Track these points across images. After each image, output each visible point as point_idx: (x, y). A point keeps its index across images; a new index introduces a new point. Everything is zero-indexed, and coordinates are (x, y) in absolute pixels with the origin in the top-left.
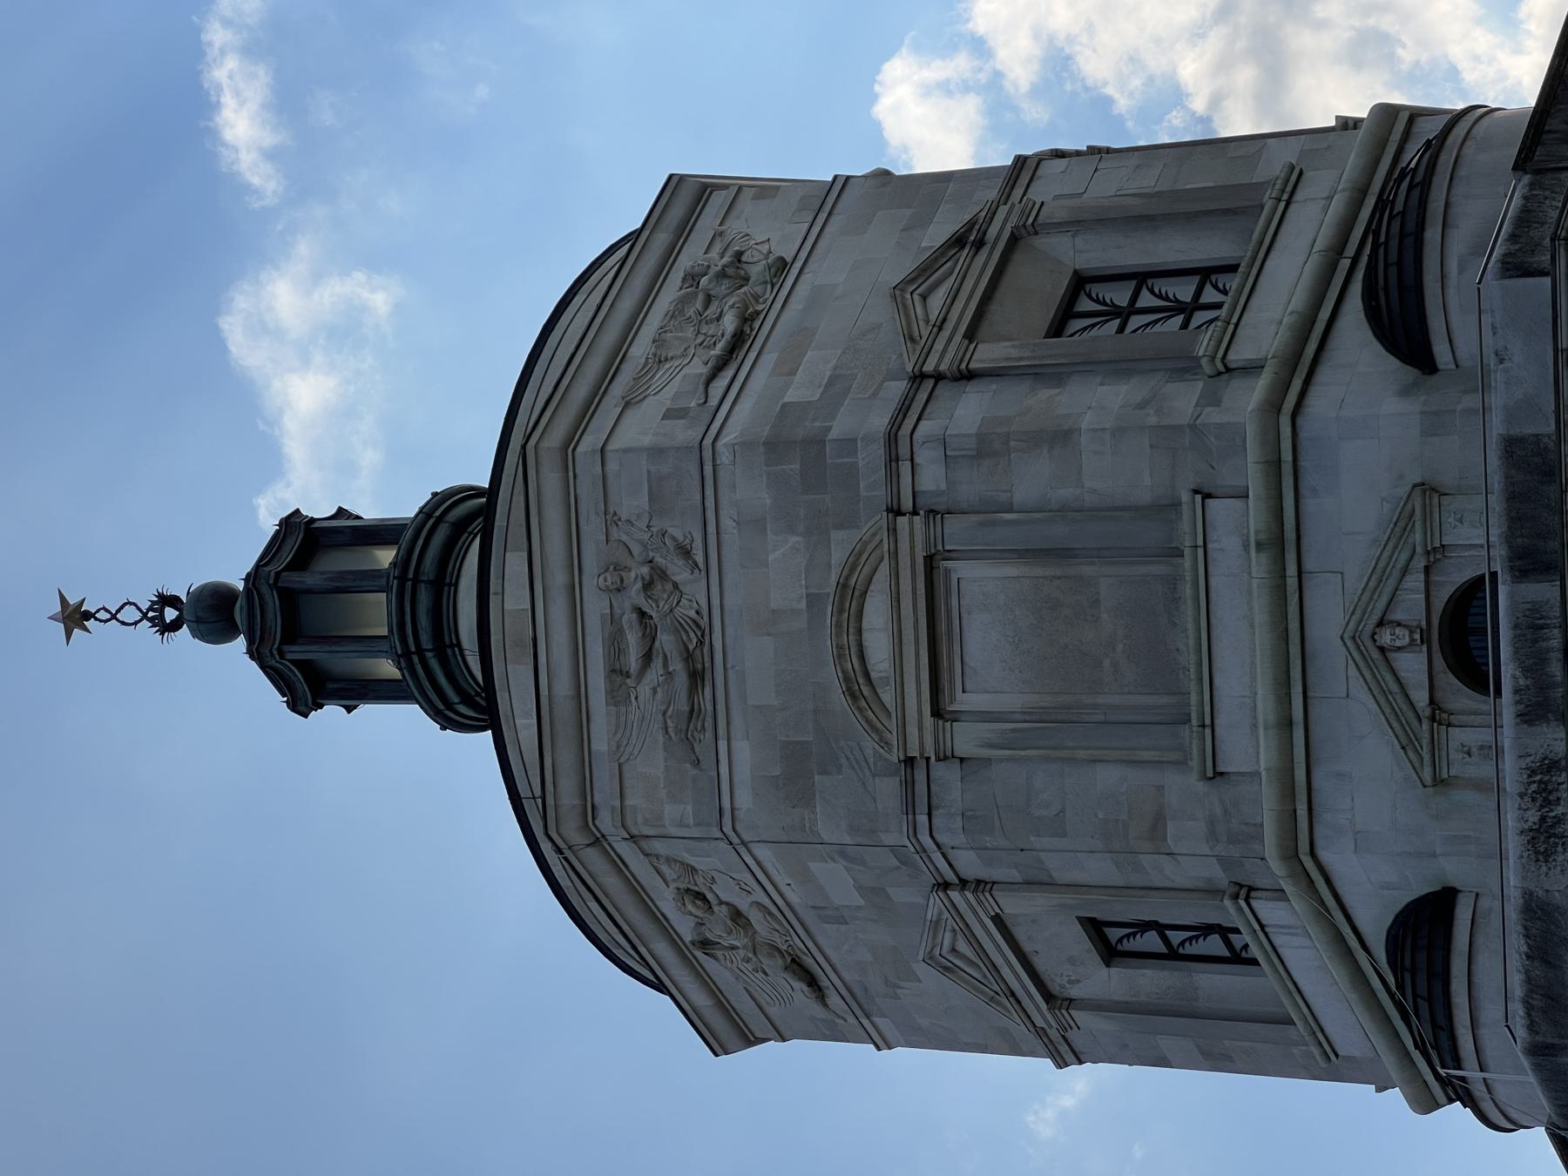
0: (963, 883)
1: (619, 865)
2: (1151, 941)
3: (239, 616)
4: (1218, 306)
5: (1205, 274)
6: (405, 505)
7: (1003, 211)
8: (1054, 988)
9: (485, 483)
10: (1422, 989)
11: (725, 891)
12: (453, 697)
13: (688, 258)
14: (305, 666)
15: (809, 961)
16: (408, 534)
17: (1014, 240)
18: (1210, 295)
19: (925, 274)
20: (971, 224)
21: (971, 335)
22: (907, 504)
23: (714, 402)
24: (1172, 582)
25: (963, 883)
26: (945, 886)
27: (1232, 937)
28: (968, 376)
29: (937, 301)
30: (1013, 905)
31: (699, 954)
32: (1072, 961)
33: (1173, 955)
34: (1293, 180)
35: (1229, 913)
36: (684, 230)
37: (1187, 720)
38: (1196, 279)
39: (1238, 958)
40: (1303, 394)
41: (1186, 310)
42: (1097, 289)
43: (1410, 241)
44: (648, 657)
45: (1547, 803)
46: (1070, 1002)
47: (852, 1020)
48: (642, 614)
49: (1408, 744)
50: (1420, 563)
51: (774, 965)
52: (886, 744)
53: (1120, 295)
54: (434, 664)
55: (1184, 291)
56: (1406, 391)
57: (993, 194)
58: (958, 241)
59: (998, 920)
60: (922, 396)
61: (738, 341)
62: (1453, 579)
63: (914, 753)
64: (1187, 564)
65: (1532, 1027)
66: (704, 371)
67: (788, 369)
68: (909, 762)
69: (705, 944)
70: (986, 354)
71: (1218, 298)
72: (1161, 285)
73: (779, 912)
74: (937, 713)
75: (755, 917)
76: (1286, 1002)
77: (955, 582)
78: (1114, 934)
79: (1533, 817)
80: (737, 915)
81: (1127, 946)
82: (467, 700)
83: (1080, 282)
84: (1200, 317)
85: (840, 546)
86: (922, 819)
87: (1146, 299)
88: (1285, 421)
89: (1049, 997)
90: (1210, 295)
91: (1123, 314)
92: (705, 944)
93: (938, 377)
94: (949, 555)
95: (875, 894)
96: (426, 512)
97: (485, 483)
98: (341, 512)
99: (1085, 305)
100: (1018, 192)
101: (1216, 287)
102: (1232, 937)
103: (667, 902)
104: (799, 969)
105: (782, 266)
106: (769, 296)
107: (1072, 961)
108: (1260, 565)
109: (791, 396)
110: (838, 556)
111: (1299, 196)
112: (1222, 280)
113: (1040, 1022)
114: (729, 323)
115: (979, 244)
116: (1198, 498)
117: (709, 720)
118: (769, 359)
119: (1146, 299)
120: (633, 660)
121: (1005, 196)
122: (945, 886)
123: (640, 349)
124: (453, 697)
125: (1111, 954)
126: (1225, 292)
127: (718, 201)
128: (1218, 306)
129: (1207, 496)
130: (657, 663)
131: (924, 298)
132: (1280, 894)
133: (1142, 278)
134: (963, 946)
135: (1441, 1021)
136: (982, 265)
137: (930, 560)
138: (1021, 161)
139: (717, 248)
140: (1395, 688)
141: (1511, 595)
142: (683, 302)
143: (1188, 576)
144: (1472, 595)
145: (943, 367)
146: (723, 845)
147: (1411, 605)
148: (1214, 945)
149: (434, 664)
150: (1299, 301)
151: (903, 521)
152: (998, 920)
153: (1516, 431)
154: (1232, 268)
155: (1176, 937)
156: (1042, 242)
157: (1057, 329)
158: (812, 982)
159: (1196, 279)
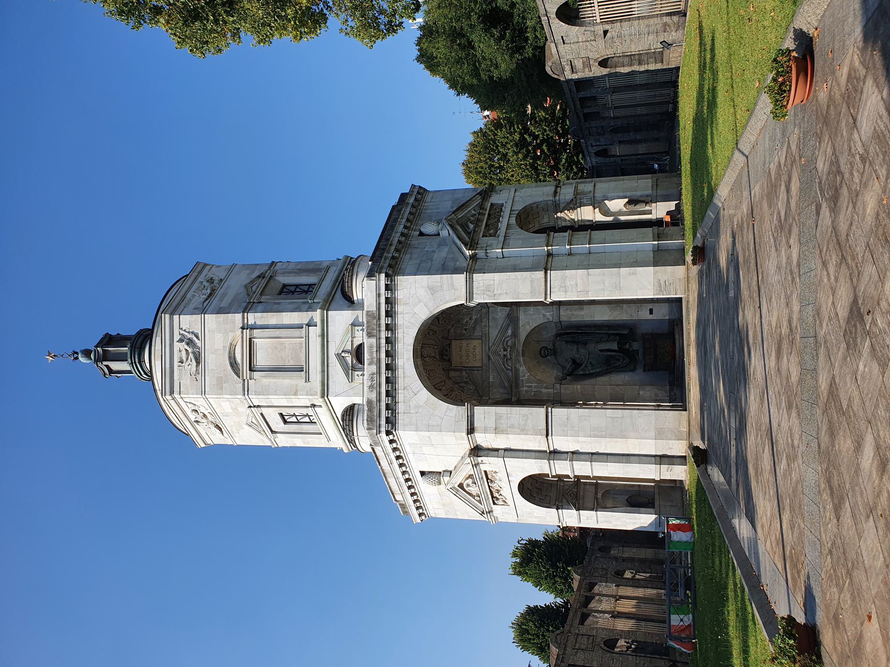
0: (255, 406)
1: (178, 404)
2: (294, 419)
3: (92, 356)
5: (310, 285)
6: (133, 332)
7: (269, 271)
8: (273, 430)
9: (151, 328)
10: (347, 424)
11: (202, 410)
12: (142, 373)
13: (200, 279)
14: (107, 366)
15: (220, 426)
16: (134, 338)
17: (271, 277)
18: (311, 289)
19: (252, 282)
20: (262, 274)
21: (261, 294)
22: (246, 327)
23: (205, 306)
24: (301, 344)
25: (255, 406)
26: (250, 407)
27: (311, 417)
28: (261, 302)
29: (254, 288)
30: (265, 411)
31: (195, 424)
32: (277, 423)
33: (298, 422)
34: (328, 269)
35: (310, 411)
36: (200, 273)
37: (303, 371)
38: (308, 287)
39: (311, 422)
40: (329, 307)
42: (287, 287)
43: (350, 278)
44: (187, 359)
45: (372, 381)
46: (276, 432)
47: (229, 438)
48: (186, 350)
49: (347, 374)
50: (350, 340)
51: (212, 427)
52: (239, 377)
53: (293, 289)
54: (138, 365)
56: (348, 307)
57: (267, 268)
58: (259, 277)
59: (262, 414)
60: (250, 306)
61: (210, 295)
62: (356, 344)
64: (304, 339)
65: (368, 424)
66: (204, 300)
67: (221, 300)
69: (197, 422)
70: (263, 299)
72: (301, 287)
73: (214, 413)
74: (251, 370)
75: (208, 415)
76: (321, 430)
78: (286, 418)
79: (370, 383)
80: (205, 415)
81: (288, 421)
82: (146, 374)
83: (284, 286)
85: (230, 336)
86: (246, 392)
89: (272, 432)
90: (311, 289)
91: (293, 292)
92: (197, 422)
93: (254, 303)
94: (254, 338)
95: (235, 409)
96: (138, 333)
97: (151, 328)
98: (118, 334)
100: (272, 268)
102: (311, 417)
103: (189, 412)
104: (217, 427)
105: (221, 280)
106: (218, 286)
107: (277, 423)
108: (319, 340)
109: (221, 306)
110: (230, 338)
111: (329, 271)
112: (313, 286)
113: (269, 437)
114: (209, 291)
115: (264, 277)
117: (200, 373)
118: (217, 299)
119: (298, 290)
120: (184, 359)
121: (269, 269)
122: (250, 407)
123: (189, 296)
124: (142, 373)
125: (285, 422)
127: (208, 268)
128: (312, 291)
129: (309, 326)
130: (189, 360)
131: (251, 287)
132: (321, 406)
133: (297, 286)
134: (254, 421)
135: (351, 430)
136: (265, 281)
138: (273, 262)
139: (207, 277)
140: (345, 364)
141: (367, 341)
142: (199, 287)
143: (304, 342)
144: (360, 347)
145: (255, 301)
146: (202, 399)
147: (349, 347)
148: (307, 419)
149: (138, 365)
150: (329, 290)
151: (245, 331)
152: (262, 414)
153: (368, 310)
154: (315, 285)
155: (299, 418)
156: (276, 278)
157: (280, 294)
158: (220, 429)
159: (308, 287)
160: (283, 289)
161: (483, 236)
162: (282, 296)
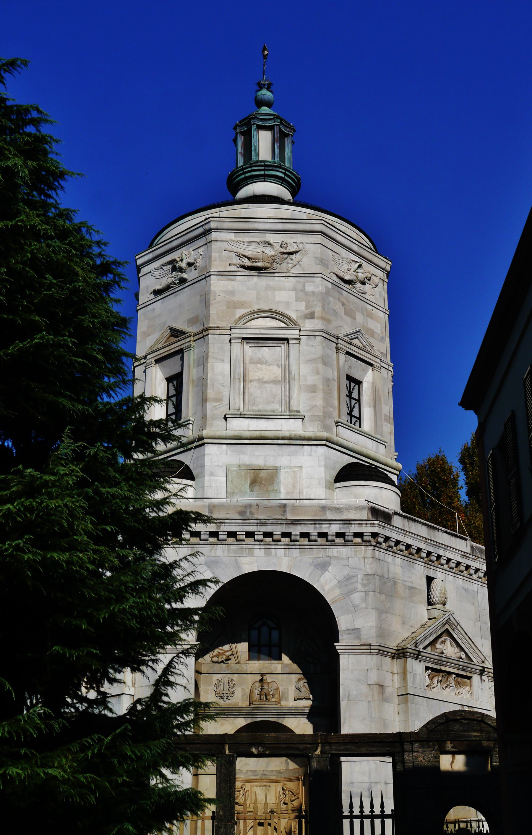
4: (351, 423)
5: (359, 419)
18: (354, 420)
21: (348, 353)
41: (350, 414)
42: (357, 387)
53: (355, 395)
55: (355, 413)
63: (233, 331)
68: (230, 330)
71: (353, 422)
72: (357, 405)
74: (244, 339)
77: (279, 345)
81: (171, 385)
83: (359, 383)
84: (349, 417)
87: (353, 402)
88: (324, 442)
90: (354, 420)
91: (350, 396)
99: (353, 384)
101: (356, 421)
112: (358, 423)
116: (303, 417)
119: (353, 402)
126: (354, 424)
133: (359, 401)
137: (287, 340)
154: (360, 427)
160: (354, 382)
161: (427, 668)
162: (344, 382)
